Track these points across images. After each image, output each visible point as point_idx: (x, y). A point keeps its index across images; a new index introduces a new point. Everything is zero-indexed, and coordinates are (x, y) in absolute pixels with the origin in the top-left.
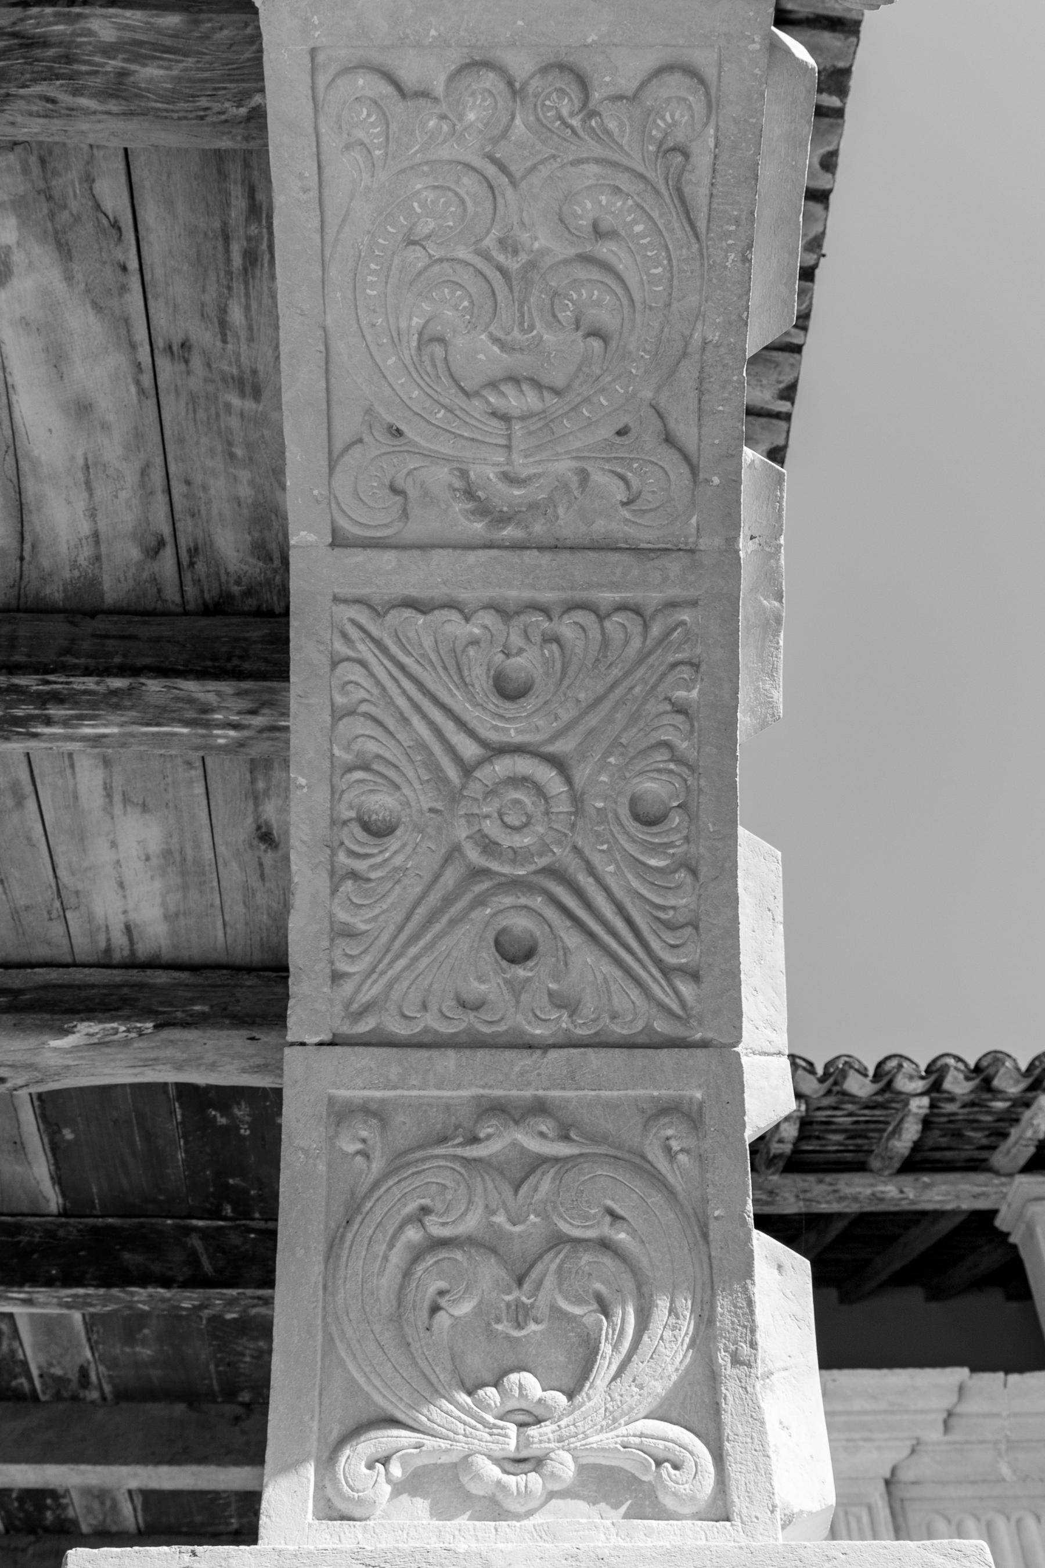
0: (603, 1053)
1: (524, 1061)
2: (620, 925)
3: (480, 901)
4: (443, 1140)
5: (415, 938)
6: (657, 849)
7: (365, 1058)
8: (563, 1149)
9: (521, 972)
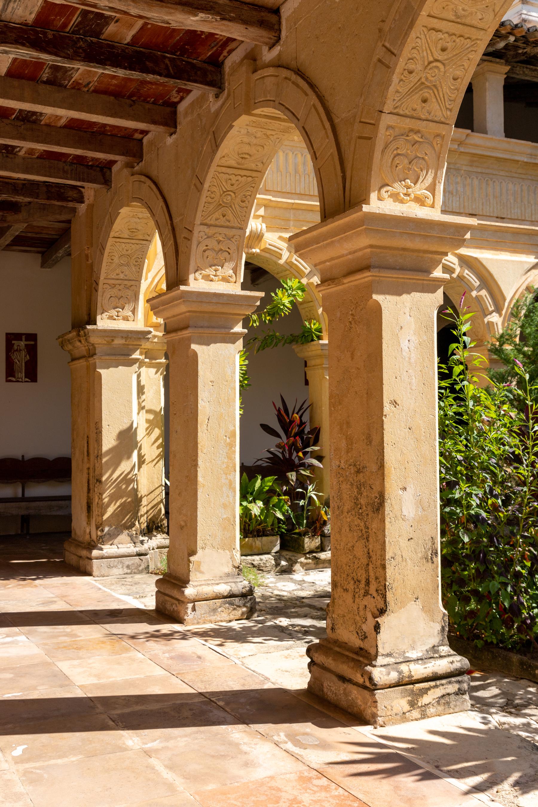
0: (433, 123)
1: (419, 122)
2: (442, 99)
3: (421, 90)
4: (402, 135)
5: (409, 95)
6: (453, 85)
7: (395, 117)
8: (421, 140)
9: (424, 105)
